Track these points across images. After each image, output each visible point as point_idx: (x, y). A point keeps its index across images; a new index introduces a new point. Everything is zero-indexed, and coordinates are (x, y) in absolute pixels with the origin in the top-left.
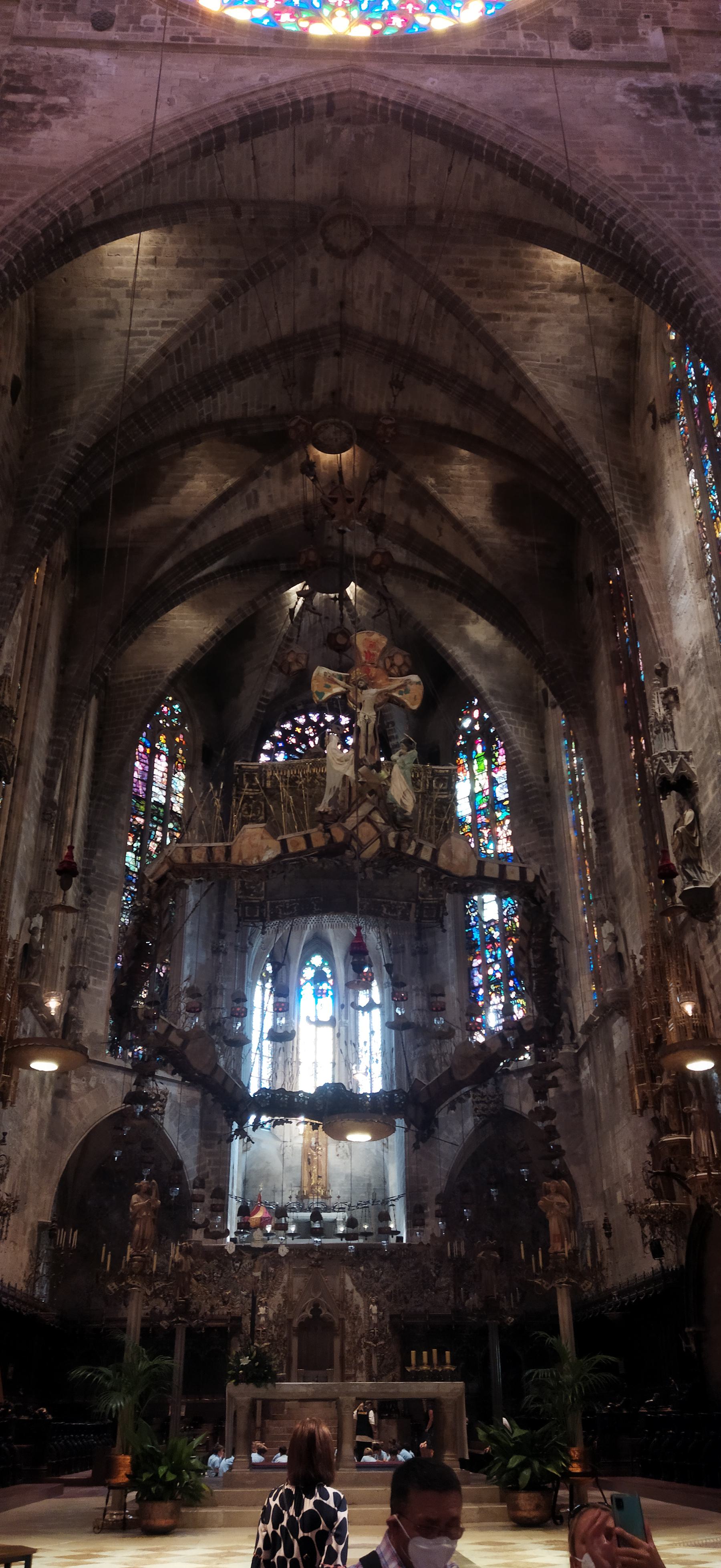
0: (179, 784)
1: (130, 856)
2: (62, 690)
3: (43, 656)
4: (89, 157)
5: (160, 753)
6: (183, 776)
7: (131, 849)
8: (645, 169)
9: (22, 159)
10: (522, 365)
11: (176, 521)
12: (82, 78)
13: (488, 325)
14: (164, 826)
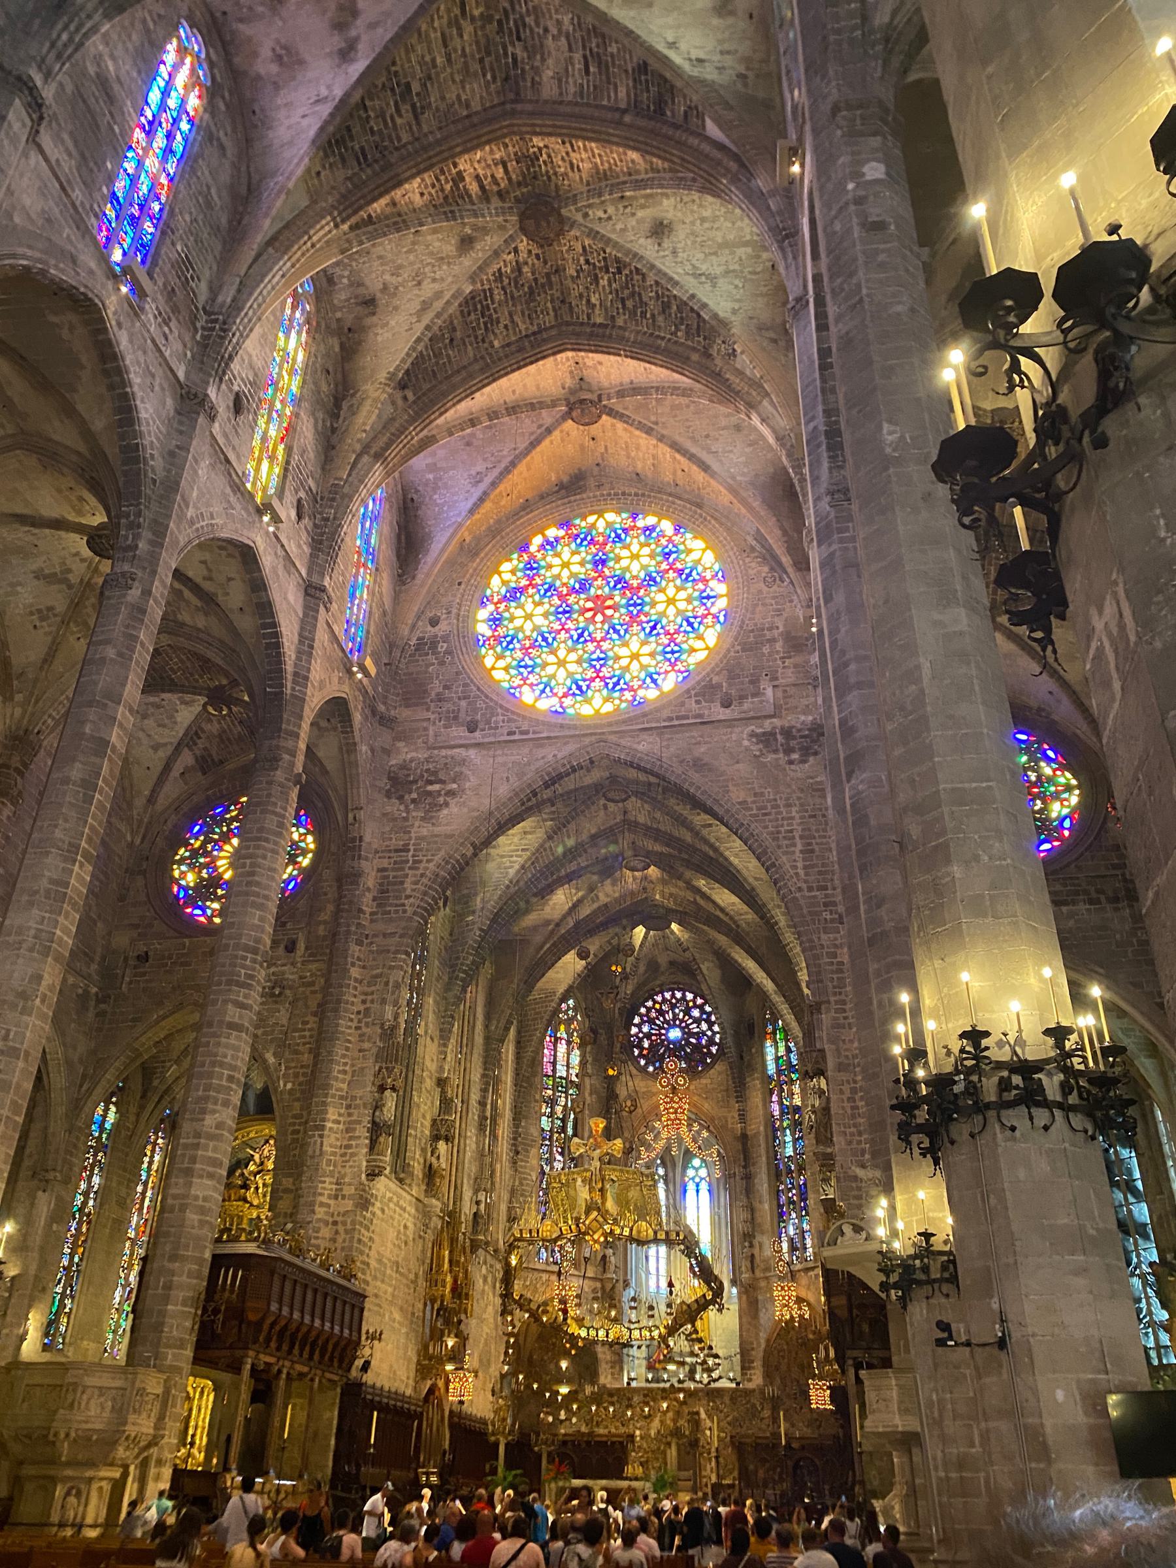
0: (575, 1059)
1: (544, 1118)
2: (487, 1039)
6: (577, 1052)
8: (755, 795)
9: (437, 830)
10: (727, 853)
11: (547, 922)
12: (464, 769)
13: (705, 832)
14: (566, 1092)
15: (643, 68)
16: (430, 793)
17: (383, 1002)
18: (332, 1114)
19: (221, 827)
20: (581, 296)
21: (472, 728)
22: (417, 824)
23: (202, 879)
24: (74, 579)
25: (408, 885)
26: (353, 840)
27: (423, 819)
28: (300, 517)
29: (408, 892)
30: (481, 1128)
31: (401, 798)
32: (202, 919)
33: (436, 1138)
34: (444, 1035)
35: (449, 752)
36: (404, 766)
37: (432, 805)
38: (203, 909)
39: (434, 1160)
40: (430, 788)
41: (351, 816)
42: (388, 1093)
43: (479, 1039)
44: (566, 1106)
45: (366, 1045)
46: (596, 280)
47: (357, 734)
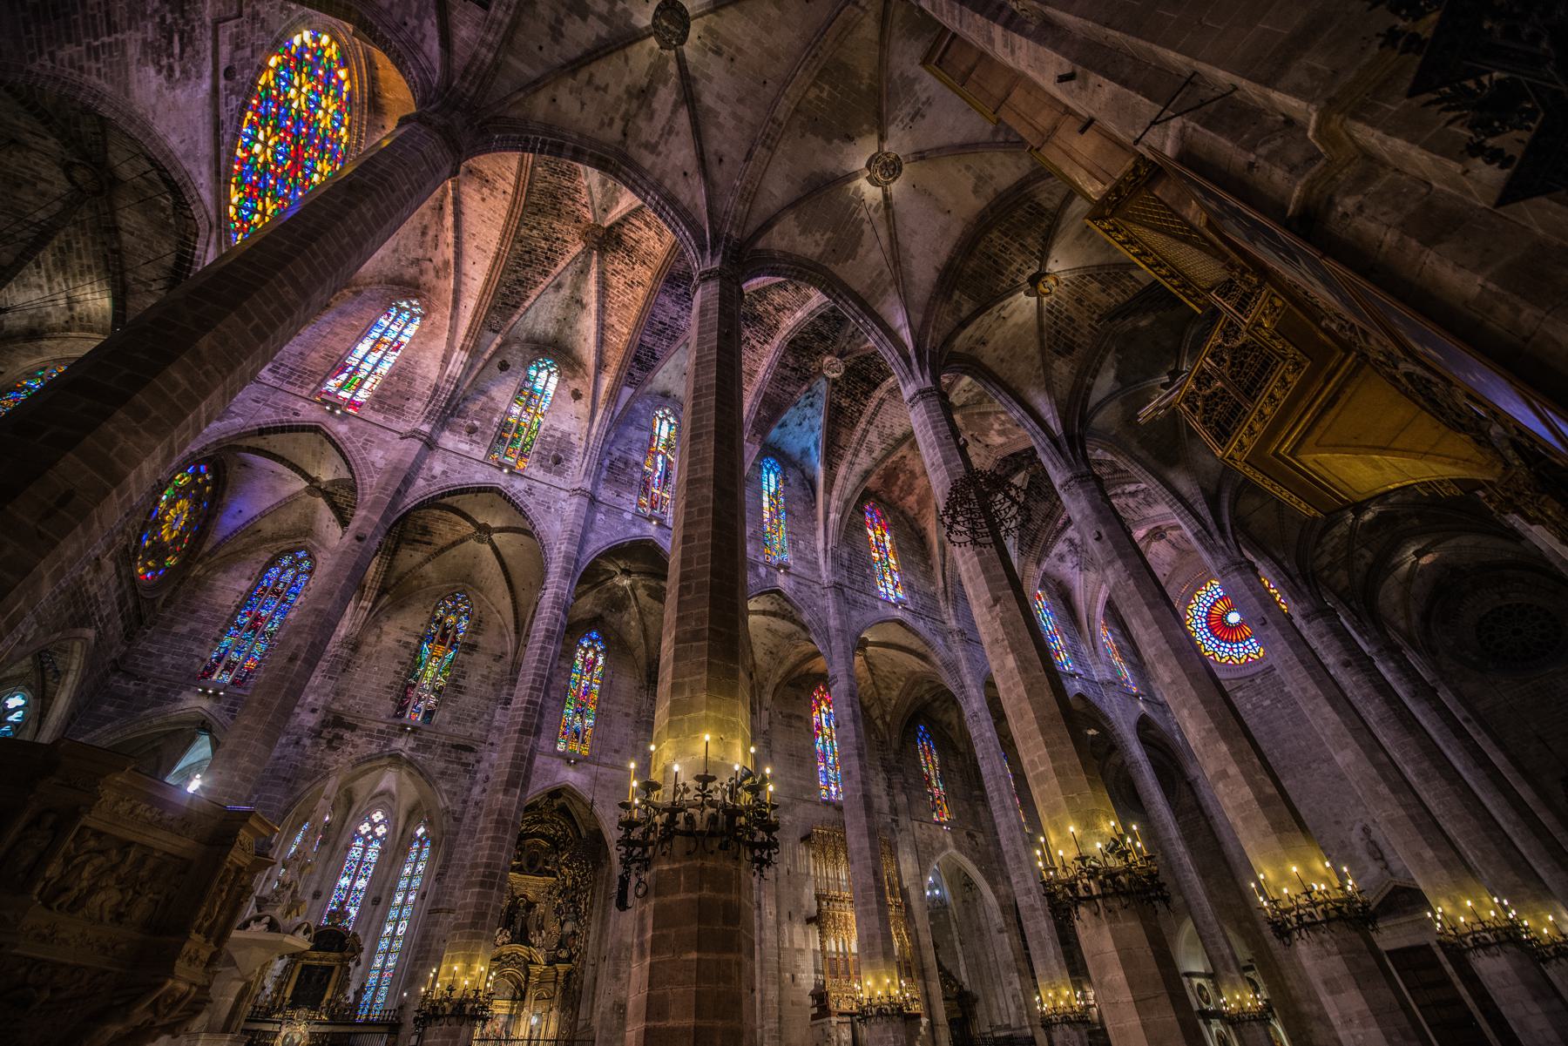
9: (133, 68)
15: (654, 357)
16: (170, 42)
20: (539, 224)
22: (139, 35)
27: (144, 41)
29: (60, 54)
35: (209, 53)
40: (176, 38)
46: (546, 240)
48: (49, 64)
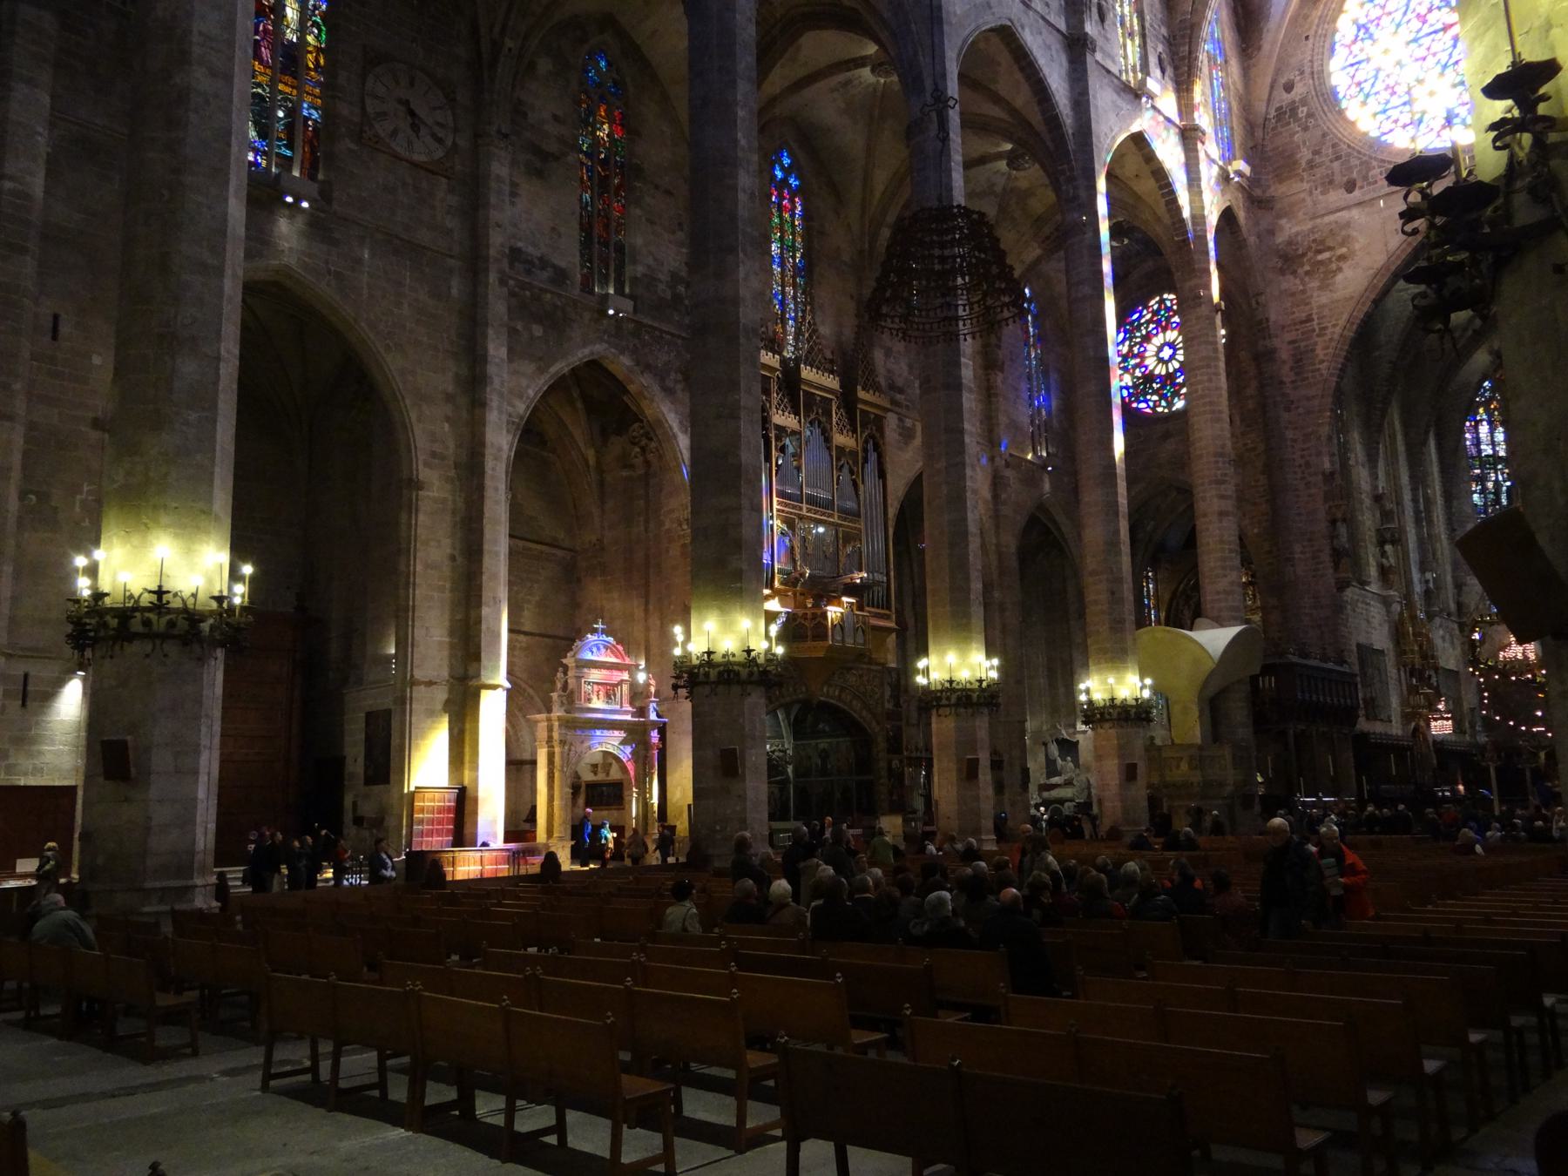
0: (1500, 436)
1: (1476, 497)
3: (1395, 438)
4: (1366, 284)
5: (1481, 420)
6: (1501, 429)
7: (1475, 492)
9: (1335, 296)
16: (1321, 262)
17: (1319, 454)
18: (1297, 548)
19: (1140, 331)
21: (1350, 187)
22: (1315, 294)
23: (1139, 378)
24: (998, 189)
25: (1320, 352)
26: (1260, 322)
27: (1320, 288)
28: (1163, 71)
29: (1321, 357)
30: (1418, 521)
31: (1294, 273)
32: (1148, 410)
33: (1381, 543)
34: (1372, 459)
35: (1332, 218)
36: (1290, 243)
37: (1326, 273)
38: (1146, 401)
39: (1384, 561)
40: (1320, 257)
41: (1254, 302)
42: (1339, 524)
43: (1401, 448)
44: (1496, 482)
45: (1313, 491)
47: (1244, 230)
48: (1325, 364)
